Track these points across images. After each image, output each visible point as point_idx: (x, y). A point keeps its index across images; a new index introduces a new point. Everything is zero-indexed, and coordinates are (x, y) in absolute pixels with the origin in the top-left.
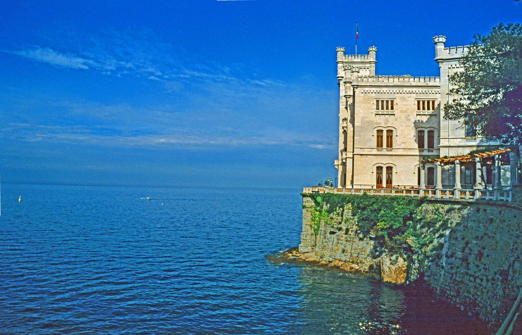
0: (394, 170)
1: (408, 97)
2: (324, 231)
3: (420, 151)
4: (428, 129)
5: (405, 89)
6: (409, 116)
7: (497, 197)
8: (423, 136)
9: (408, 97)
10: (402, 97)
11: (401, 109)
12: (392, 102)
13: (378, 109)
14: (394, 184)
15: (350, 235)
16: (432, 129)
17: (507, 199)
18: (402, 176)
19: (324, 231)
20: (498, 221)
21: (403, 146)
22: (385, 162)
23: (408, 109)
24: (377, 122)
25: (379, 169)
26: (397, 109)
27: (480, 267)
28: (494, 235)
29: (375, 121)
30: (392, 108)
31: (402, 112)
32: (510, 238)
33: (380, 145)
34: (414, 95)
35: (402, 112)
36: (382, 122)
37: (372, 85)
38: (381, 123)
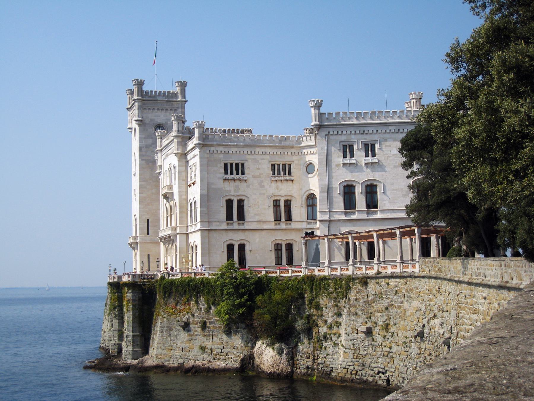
0: (247, 248)
1: (261, 159)
2: (167, 327)
3: (276, 224)
4: (285, 198)
5: (257, 150)
6: (262, 181)
7: (401, 269)
8: (280, 206)
9: (261, 159)
10: (254, 159)
11: (253, 174)
12: (243, 165)
13: (226, 173)
14: (248, 264)
15: (209, 327)
16: (289, 198)
17: (413, 270)
18: (257, 254)
19: (167, 327)
20: (404, 291)
21: (257, 218)
22: (236, 239)
23: (262, 174)
24: (227, 189)
25: (230, 248)
26: (248, 174)
27: (387, 337)
28: (400, 304)
29: (224, 189)
30: (243, 173)
31: (254, 177)
32: (421, 303)
33: (229, 217)
34: (268, 157)
35: (254, 177)
36: (232, 189)
37: (219, 143)
38: (230, 191)
